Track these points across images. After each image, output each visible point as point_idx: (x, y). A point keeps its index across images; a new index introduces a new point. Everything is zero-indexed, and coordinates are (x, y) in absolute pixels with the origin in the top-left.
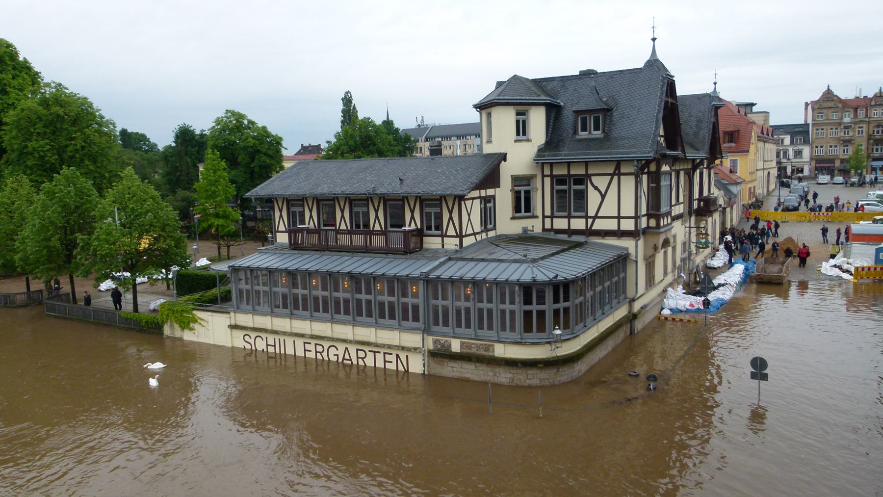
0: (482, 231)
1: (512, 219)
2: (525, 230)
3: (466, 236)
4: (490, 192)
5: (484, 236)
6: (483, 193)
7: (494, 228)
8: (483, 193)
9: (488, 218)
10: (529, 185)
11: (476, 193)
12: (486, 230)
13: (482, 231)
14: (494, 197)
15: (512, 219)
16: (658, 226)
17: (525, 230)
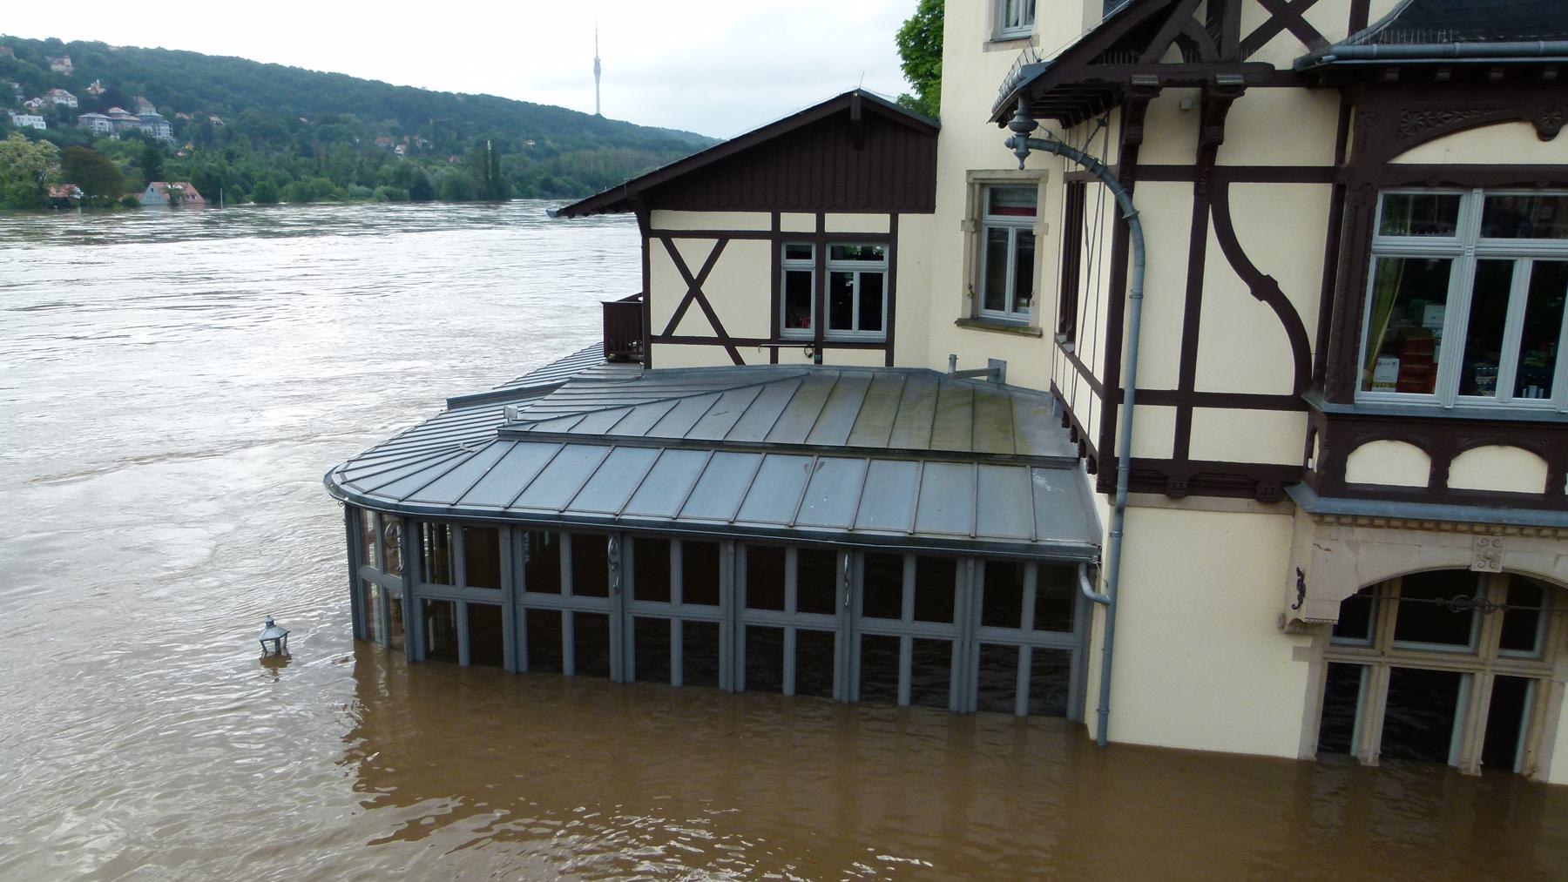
0: (775, 342)
1: (961, 323)
2: (996, 371)
3: (668, 337)
4: (838, 223)
5: (793, 357)
6: (799, 222)
7: (888, 345)
8: (799, 222)
9: (836, 298)
10: (1032, 212)
11: (762, 220)
12: (818, 345)
13: (775, 342)
14: (891, 239)
15: (961, 323)
16: (1331, 480)
17: (996, 371)
